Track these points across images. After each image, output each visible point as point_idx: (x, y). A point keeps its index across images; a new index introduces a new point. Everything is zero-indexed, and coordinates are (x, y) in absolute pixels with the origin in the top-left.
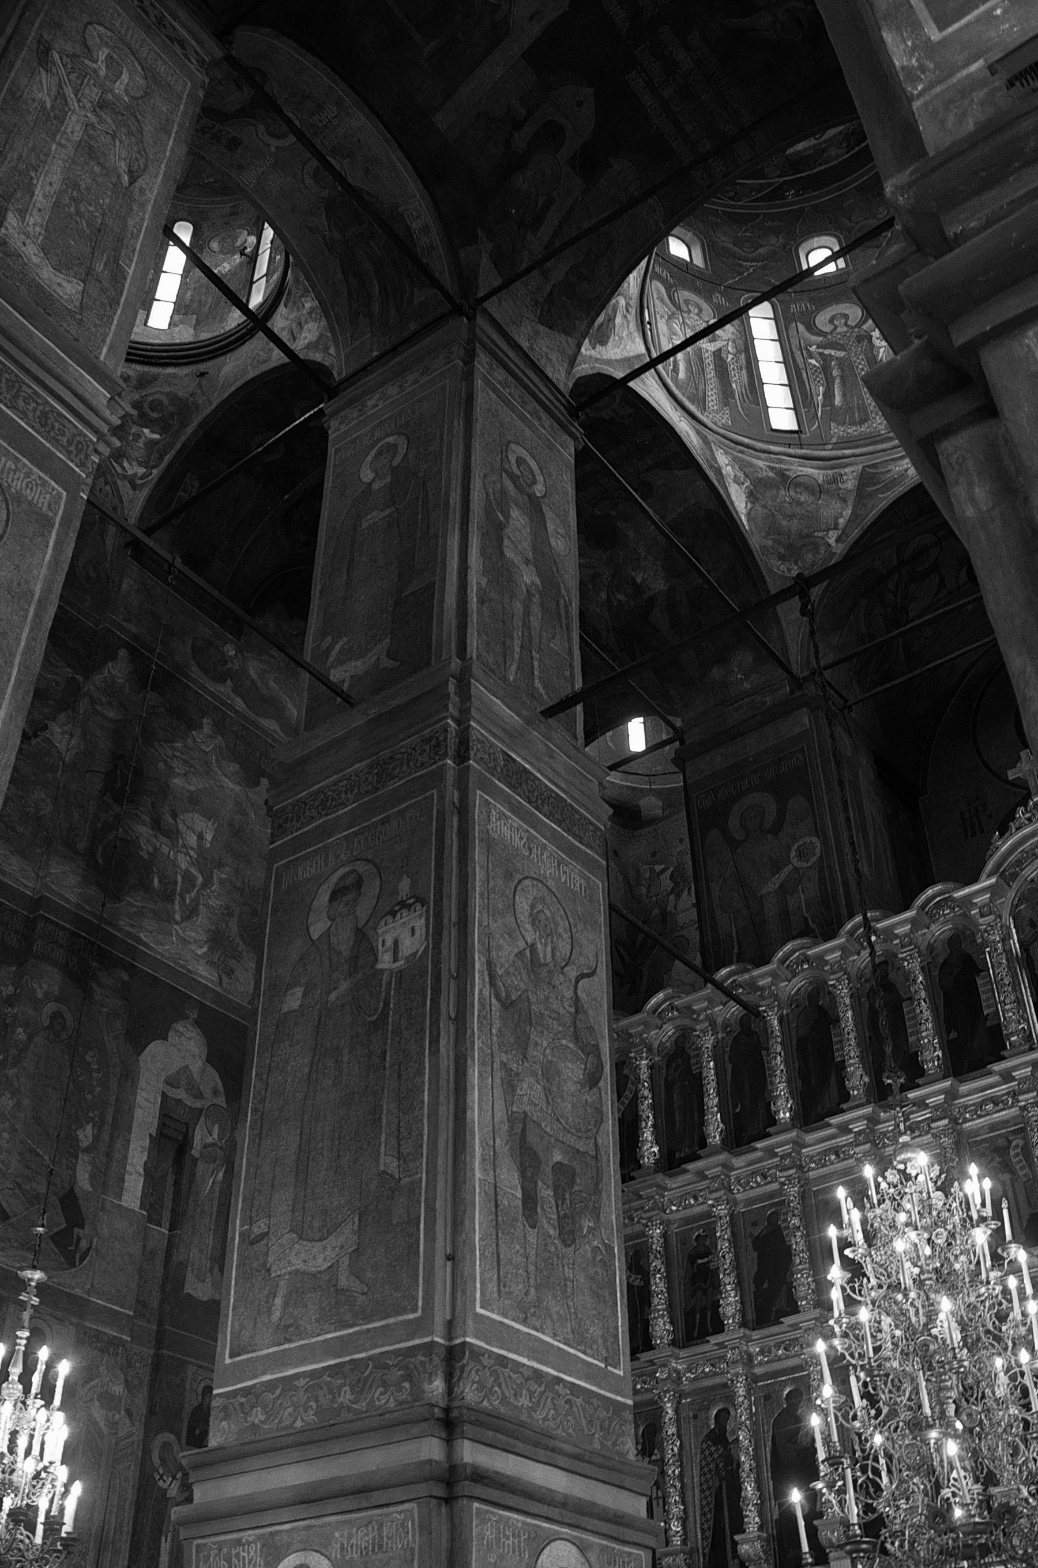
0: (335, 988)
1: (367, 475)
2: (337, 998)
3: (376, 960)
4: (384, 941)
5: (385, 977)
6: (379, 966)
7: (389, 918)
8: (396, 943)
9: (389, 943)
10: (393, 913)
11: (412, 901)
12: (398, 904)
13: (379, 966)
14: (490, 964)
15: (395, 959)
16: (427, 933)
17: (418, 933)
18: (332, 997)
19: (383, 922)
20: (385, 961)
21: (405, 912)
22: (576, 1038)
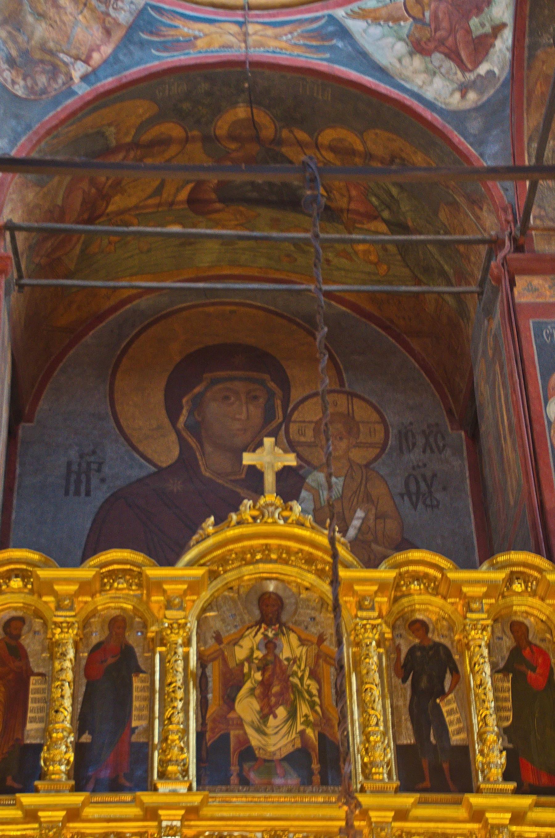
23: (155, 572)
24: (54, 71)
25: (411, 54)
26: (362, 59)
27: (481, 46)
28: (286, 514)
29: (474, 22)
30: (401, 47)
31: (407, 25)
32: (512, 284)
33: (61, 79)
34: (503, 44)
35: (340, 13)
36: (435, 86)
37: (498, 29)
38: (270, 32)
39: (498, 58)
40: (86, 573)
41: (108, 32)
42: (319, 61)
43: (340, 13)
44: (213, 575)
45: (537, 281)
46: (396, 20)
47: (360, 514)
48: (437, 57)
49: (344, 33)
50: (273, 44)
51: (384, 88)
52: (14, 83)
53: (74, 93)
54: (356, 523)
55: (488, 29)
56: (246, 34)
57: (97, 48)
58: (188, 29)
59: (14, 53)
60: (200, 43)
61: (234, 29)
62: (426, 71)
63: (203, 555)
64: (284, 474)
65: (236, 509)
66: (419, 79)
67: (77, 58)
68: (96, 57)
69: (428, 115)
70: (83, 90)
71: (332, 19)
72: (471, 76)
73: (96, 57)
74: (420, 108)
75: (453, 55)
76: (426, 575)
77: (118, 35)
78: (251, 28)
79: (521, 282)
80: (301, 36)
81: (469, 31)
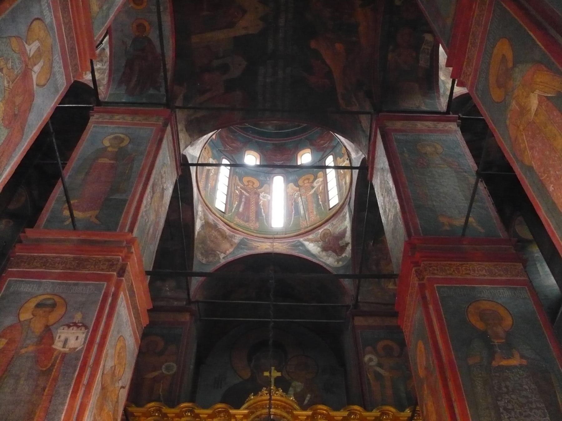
0: (26, 347)
1: (107, 143)
2: (26, 352)
3: (53, 343)
4: (60, 337)
5: (56, 353)
6: (54, 346)
7: (66, 328)
8: (66, 341)
9: (63, 338)
10: (69, 326)
11: (81, 325)
12: (73, 323)
13: (54, 346)
14: (104, 366)
15: (64, 347)
16: (85, 342)
17: (79, 340)
18: (23, 351)
19: (62, 328)
20: (58, 345)
21: (75, 328)
22: (114, 414)
23: (233, 411)
24: (215, 255)
25: (322, 251)
26: (308, 252)
27: (343, 249)
28: (277, 392)
29: (340, 242)
30: (319, 249)
31: (321, 243)
32: (353, 319)
33: (217, 258)
34: (349, 248)
35: (301, 240)
36: (329, 261)
37: (347, 244)
38: (280, 245)
39: (348, 253)
40: (209, 411)
41: (232, 245)
42: (295, 253)
43: (301, 240)
44: (252, 413)
45: (361, 318)
46: (318, 241)
47: (309, 395)
48: (330, 252)
49: (303, 245)
50: (281, 248)
51: (314, 260)
52: (202, 260)
53: (220, 262)
54: (308, 398)
55: (344, 244)
56: (273, 246)
57: (228, 250)
58: (255, 244)
59: (203, 251)
60: (259, 248)
61: (270, 244)
62: (327, 256)
63: (249, 406)
64: (277, 379)
65: (261, 391)
66: (325, 258)
67: (222, 253)
68: (228, 252)
69: (328, 268)
70: (223, 262)
71: (299, 241)
72: (341, 257)
73: (228, 252)
74: (325, 266)
75: (334, 251)
76: (323, 414)
77: (234, 246)
78: (275, 244)
79: (356, 318)
80: (289, 246)
81: (339, 245)
